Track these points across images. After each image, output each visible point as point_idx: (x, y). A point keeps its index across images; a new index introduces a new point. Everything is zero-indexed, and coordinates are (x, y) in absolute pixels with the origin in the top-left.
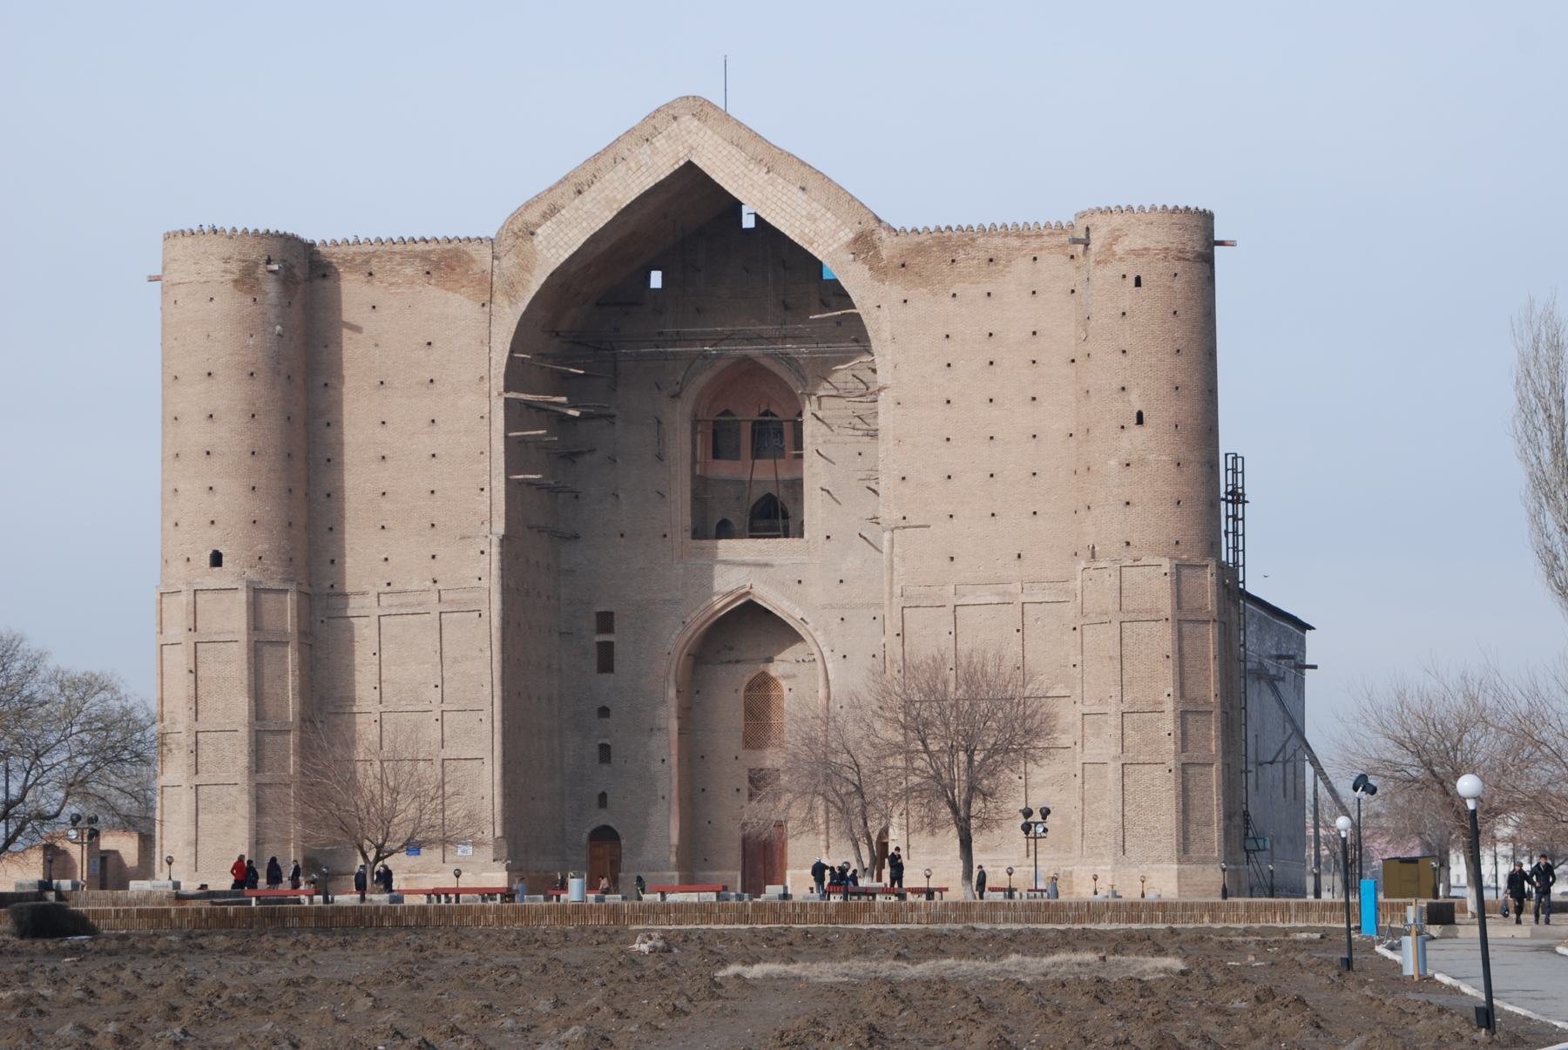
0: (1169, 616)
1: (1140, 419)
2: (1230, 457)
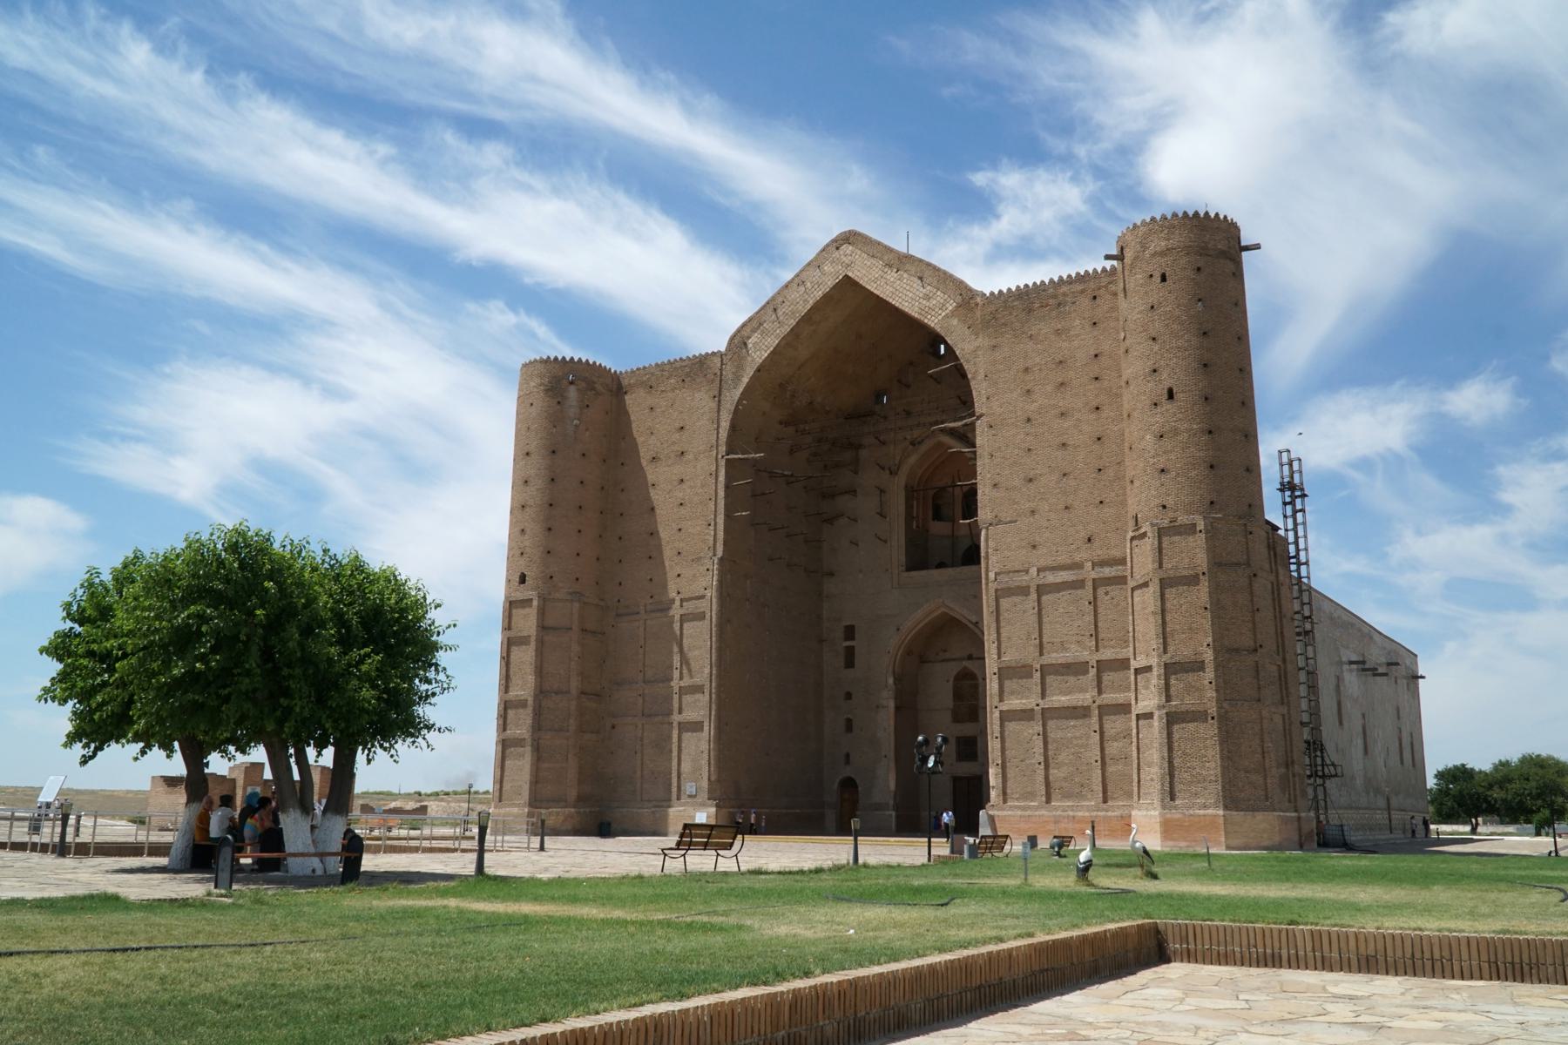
0: (1205, 570)
2: (1285, 455)
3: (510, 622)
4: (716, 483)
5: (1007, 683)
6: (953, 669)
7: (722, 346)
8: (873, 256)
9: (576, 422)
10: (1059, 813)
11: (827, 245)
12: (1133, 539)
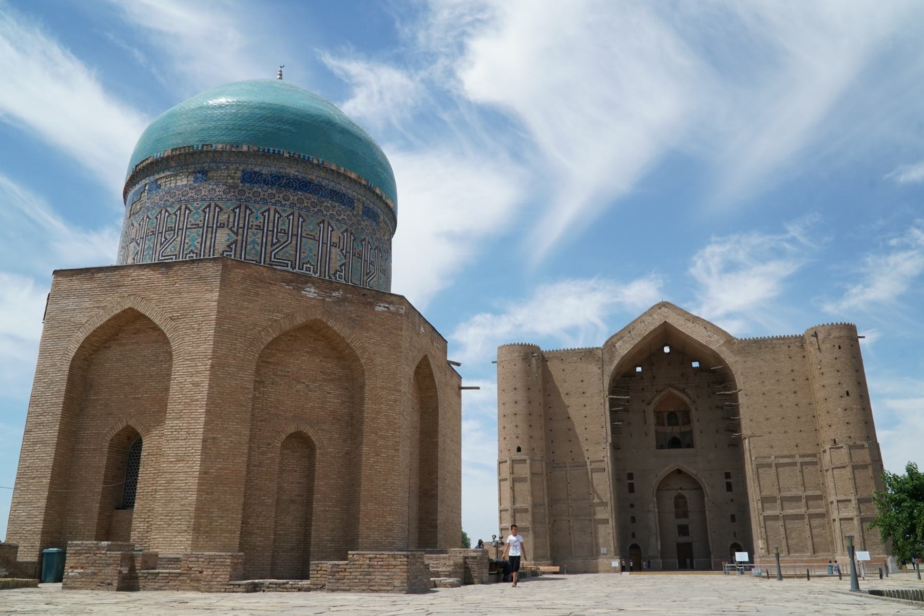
1: (848, 394)
3: (513, 470)
4: (605, 408)
5: (765, 505)
6: (673, 494)
7: (600, 344)
8: (679, 315)
9: (536, 375)
10: (795, 559)
11: (654, 306)
12: (830, 448)
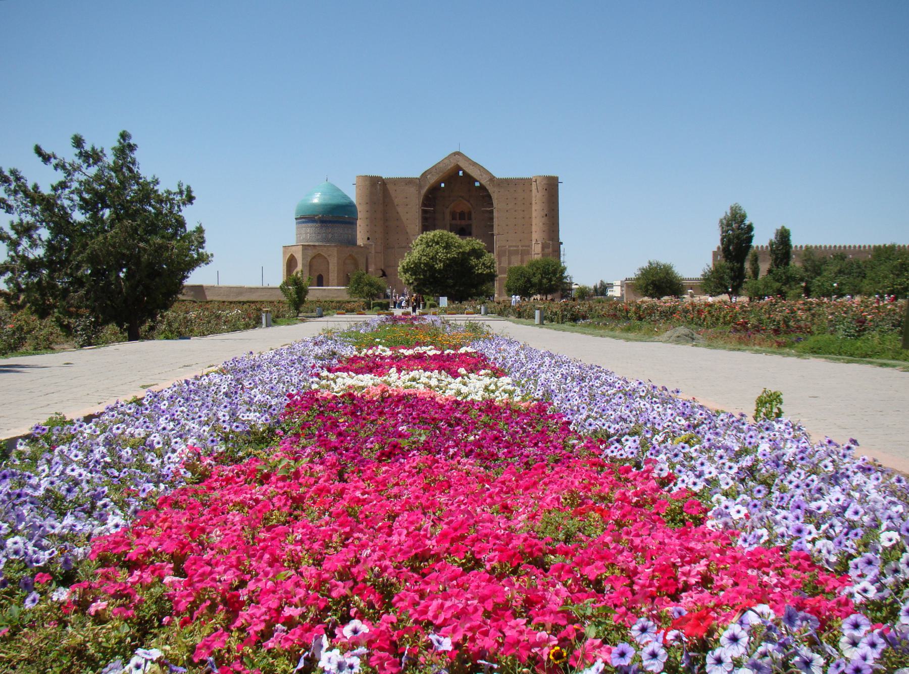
7: (418, 176)
